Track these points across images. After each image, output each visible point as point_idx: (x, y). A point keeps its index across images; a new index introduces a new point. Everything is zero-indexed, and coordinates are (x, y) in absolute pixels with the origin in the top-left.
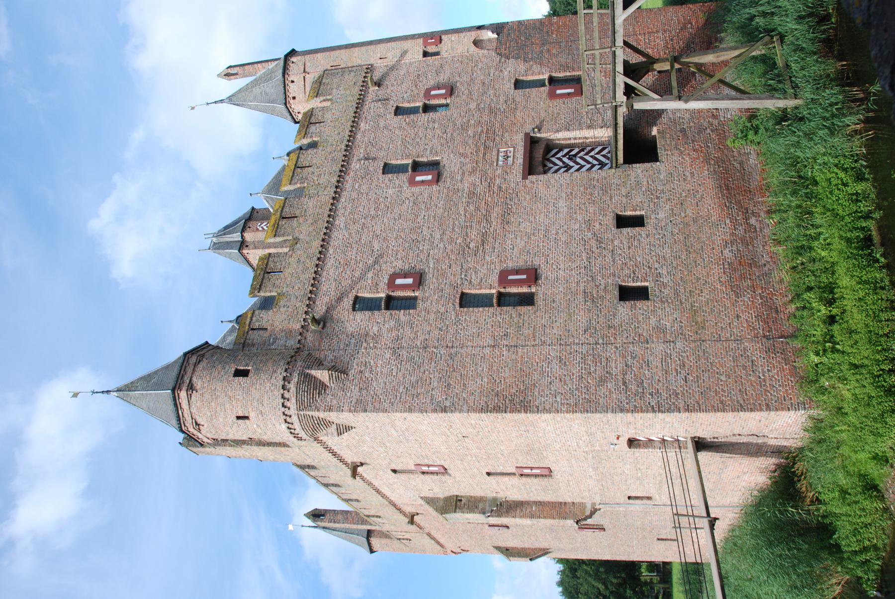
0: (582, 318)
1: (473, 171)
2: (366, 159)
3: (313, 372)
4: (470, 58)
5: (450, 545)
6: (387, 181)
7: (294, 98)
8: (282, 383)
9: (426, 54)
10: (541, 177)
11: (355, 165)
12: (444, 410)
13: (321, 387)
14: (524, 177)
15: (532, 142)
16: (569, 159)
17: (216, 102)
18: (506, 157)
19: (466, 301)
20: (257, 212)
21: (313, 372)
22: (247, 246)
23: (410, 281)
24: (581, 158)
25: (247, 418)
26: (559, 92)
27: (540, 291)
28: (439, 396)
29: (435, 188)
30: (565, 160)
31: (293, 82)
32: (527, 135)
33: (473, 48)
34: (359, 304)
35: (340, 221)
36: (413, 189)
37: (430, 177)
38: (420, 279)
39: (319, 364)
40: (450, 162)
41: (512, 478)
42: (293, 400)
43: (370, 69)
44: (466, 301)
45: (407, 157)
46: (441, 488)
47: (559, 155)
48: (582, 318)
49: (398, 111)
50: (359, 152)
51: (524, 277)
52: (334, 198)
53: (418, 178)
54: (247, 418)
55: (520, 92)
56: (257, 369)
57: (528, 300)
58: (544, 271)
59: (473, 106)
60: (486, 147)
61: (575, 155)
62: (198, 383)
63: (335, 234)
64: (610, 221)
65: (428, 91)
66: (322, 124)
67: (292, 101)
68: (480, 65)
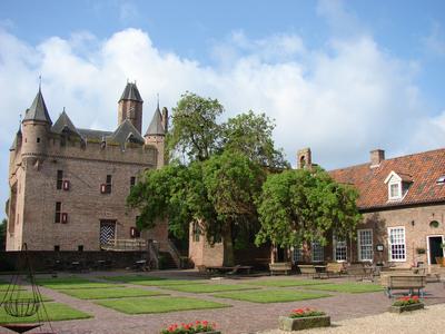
0: (50, 235)
11: (111, 166)
13: (34, 164)
15: (114, 221)
19: (58, 204)
27: (59, 225)
34: (60, 173)
39: (41, 162)
40: (108, 198)
44: (58, 204)
48: (50, 235)
57: (57, 221)
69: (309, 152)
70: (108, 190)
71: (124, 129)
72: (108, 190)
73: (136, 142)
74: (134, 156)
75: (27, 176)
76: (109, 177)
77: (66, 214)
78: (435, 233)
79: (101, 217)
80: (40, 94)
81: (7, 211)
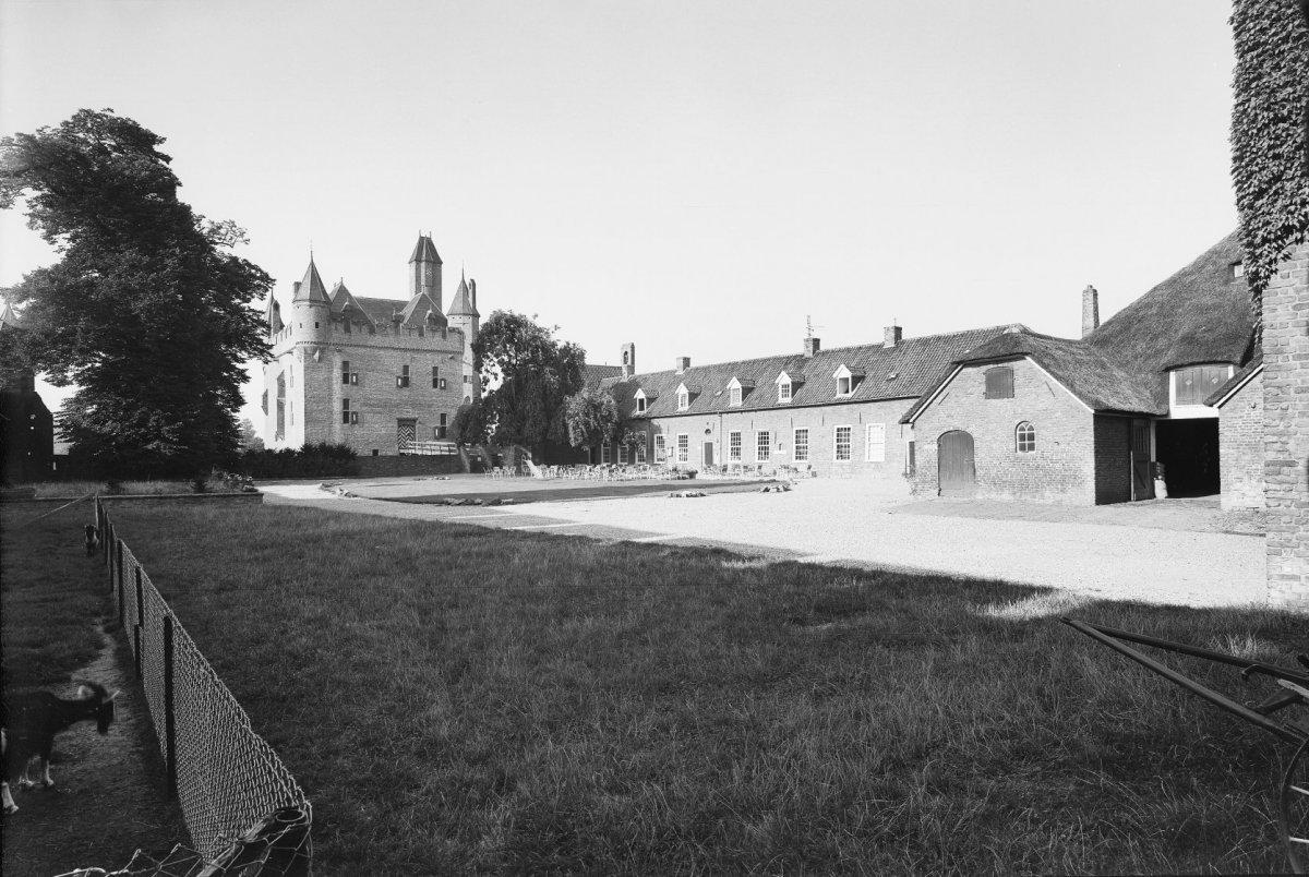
9: (465, 377)
10: (396, 425)
15: (414, 420)
34: (345, 364)
39: (322, 351)
40: (406, 392)
43: (462, 353)
49: (435, 369)
65: (445, 381)
69: (633, 347)
70: (406, 382)
71: (423, 302)
72: (406, 382)
73: (439, 322)
74: (434, 341)
75: (306, 368)
76: (406, 368)
78: (708, 438)
80: (312, 264)
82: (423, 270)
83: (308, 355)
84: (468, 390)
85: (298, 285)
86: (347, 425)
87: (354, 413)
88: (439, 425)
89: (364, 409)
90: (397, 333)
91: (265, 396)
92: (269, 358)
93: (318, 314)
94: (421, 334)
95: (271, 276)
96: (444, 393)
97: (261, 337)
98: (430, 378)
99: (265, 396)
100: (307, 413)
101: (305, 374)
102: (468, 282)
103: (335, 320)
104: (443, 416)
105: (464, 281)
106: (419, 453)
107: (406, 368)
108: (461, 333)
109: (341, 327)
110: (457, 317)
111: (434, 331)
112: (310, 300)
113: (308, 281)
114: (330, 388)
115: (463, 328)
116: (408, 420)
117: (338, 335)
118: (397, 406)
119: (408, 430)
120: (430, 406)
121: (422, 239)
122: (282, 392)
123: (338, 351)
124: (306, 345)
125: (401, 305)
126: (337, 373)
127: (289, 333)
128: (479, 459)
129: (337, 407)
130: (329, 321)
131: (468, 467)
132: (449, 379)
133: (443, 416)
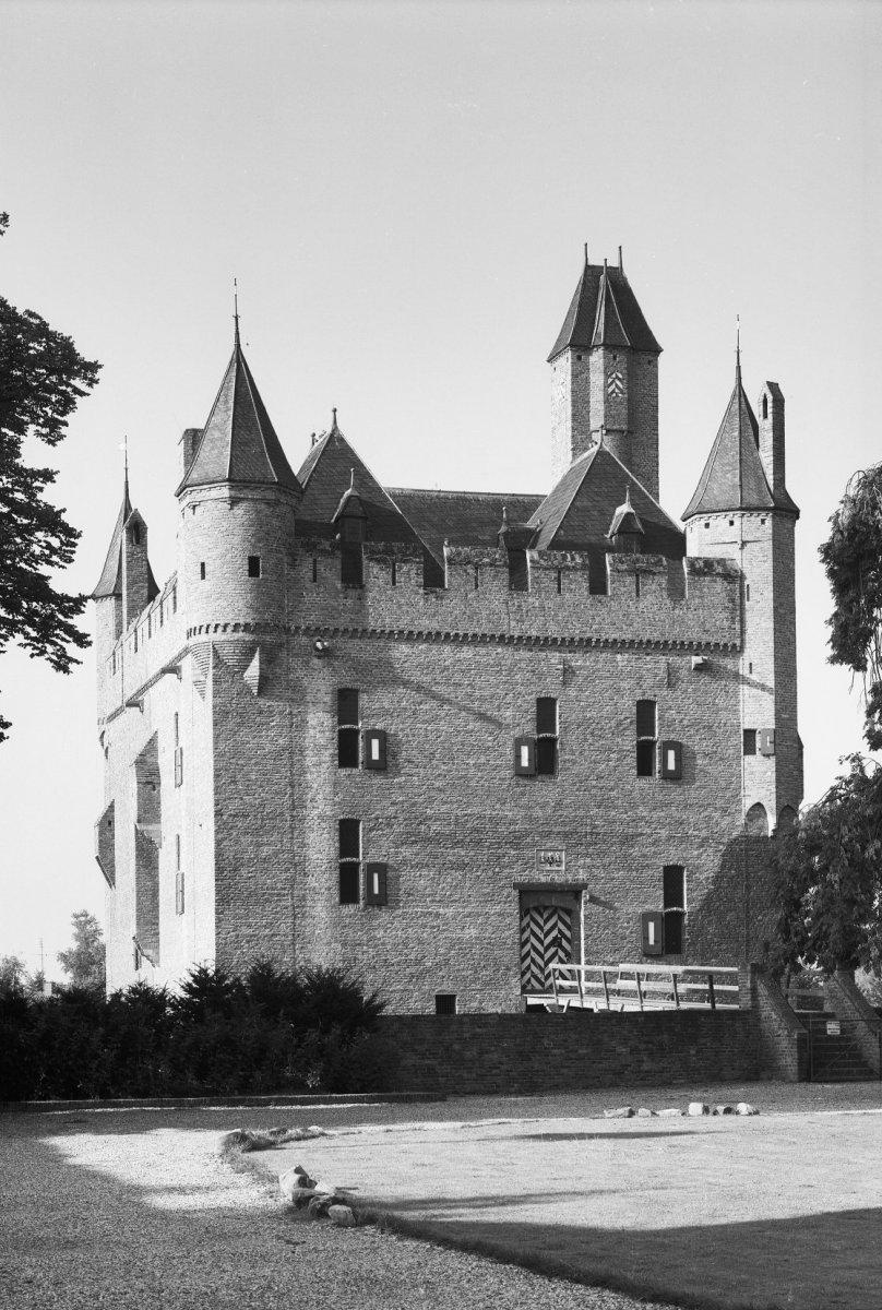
1: (530, 819)
2: (565, 671)
3: (257, 656)
4: (736, 798)
5: (113, 730)
6: (525, 706)
7: (707, 525)
8: (242, 622)
9: (750, 734)
10: (514, 908)
11: (555, 658)
12: (218, 814)
14: (516, 886)
15: (575, 891)
16: (555, 938)
17: (739, 368)
18: (551, 862)
20: (649, 362)
21: (257, 656)
22: (579, 358)
23: (375, 756)
24: (556, 953)
25: (203, 577)
26: (651, 926)
28: (234, 806)
29: (508, 773)
30: (555, 933)
31: (732, 523)
32: (585, 886)
33: (748, 803)
35: (467, 652)
36: (510, 743)
37: (525, 763)
38: (379, 768)
39: (268, 662)
41: (175, 865)
42: (224, 637)
43: (737, 650)
45: (565, 730)
46: (165, 761)
47: (560, 925)
49: (645, 709)
50: (578, 660)
51: (376, 891)
52: (502, 637)
53: (525, 751)
54: (203, 577)
55: (659, 873)
56: (259, 585)
58: (384, 916)
59: (642, 811)
60: (566, 835)
61: (560, 946)
62: (239, 510)
63: (447, 649)
64: (447, 988)
66: (634, 594)
67: (703, 522)
68: (717, 815)
70: (545, 759)
72: (545, 759)
75: (220, 716)
76: (545, 708)
77: (381, 868)
79: (523, 878)
80: (239, 360)
81: (106, 862)
82: (597, 379)
83: (225, 671)
84: (758, 780)
85: (194, 438)
86: (350, 909)
87: (372, 868)
88: (660, 907)
89: (406, 852)
90: (517, 582)
91: (107, 823)
92: (72, 649)
93: (261, 531)
94: (598, 587)
95: (86, 352)
96: (676, 793)
97: (44, 569)
98: (629, 742)
99: (107, 823)
100: (225, 869)
101: (217, 737)
102: (756, 394)
103: (310, 548)
104: (672, 877)
105: (740, 394)
106: (596, 1004)
107: (545, 708)
108: (733, 577)
109: (331, 571)
110: (720, 523)
111: (639, 573)
112: (232, 480)
113: (226, 419)
114: (295, 783)
115: (733, 553)
116: (551, 889)
117: (319, 600)
118: (516, 841)
119: (554, 926)
120: (628, 840)
121: (591, 273)
122: (149, 809)
123: (326, 654)
124: (219, 636)
125: (525, 505)
126: (319, 727)
127: (168, 603)
128: (833, 1028)
129: (320, 847)
130: (293, 556)
131: (789, 1060)
132: (697, 743)
133: (672, 877)
